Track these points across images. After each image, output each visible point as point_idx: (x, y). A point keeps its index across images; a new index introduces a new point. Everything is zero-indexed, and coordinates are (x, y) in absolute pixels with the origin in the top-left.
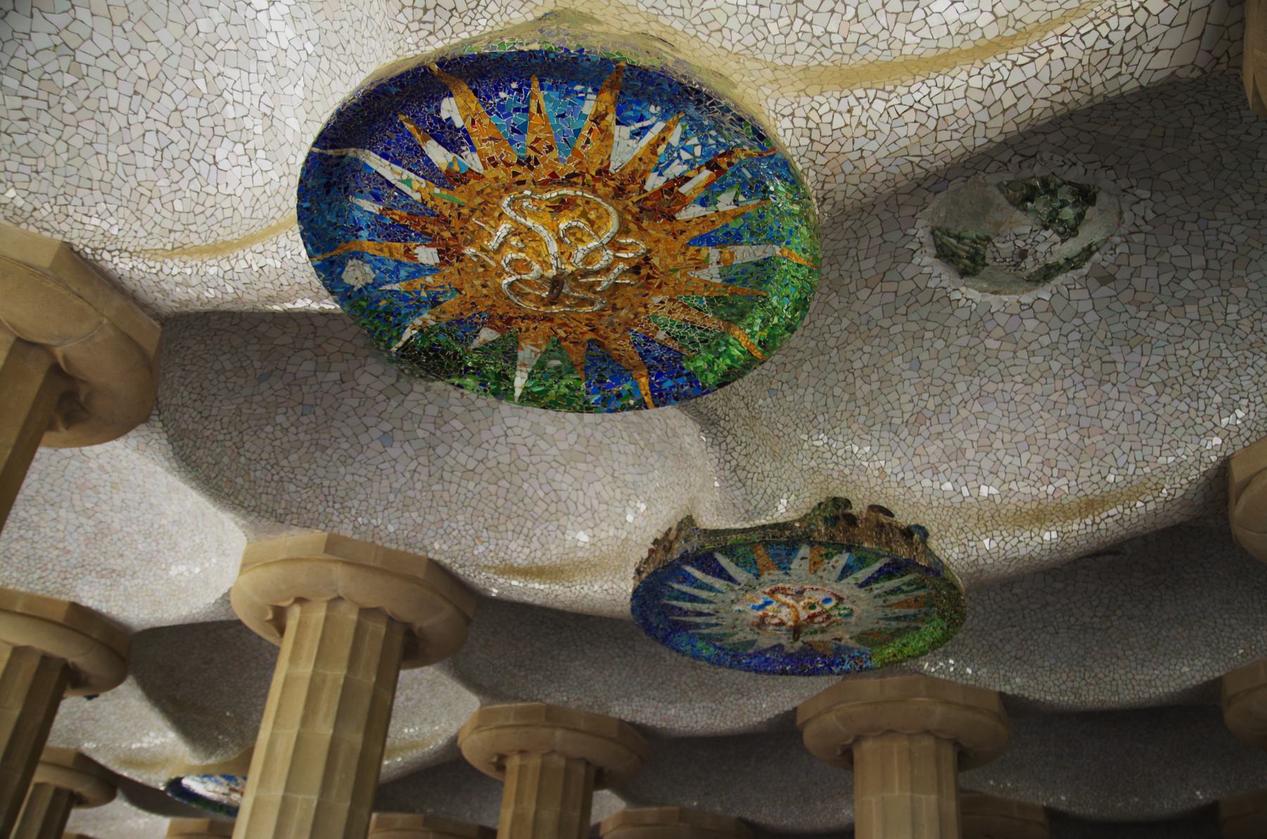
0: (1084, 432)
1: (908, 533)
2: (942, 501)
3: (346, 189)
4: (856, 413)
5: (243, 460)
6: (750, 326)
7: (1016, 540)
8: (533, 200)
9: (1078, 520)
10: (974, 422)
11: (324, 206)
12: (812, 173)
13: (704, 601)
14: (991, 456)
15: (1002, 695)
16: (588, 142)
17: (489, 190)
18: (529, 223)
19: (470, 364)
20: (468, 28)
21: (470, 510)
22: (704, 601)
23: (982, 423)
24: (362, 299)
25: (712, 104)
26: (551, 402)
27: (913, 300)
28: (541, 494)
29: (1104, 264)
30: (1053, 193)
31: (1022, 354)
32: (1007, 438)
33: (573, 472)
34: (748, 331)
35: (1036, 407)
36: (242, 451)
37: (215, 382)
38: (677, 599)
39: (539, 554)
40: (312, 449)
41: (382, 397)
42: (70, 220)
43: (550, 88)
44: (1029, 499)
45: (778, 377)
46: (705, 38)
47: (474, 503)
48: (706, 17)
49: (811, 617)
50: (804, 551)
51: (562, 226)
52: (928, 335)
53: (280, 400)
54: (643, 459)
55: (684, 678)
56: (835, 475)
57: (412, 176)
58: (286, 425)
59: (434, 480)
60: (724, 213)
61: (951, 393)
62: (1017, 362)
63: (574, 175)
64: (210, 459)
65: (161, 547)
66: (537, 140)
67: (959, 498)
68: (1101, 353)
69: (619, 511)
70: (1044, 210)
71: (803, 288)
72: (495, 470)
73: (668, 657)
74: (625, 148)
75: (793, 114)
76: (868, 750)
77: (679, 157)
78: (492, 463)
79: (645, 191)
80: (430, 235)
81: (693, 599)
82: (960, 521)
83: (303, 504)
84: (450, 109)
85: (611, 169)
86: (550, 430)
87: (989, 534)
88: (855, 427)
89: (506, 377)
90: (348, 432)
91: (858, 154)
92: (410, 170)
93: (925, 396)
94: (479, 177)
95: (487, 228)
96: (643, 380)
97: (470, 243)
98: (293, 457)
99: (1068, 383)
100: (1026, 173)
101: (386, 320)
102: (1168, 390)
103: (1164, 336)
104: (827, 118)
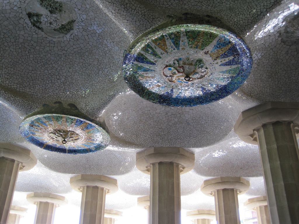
5: (211, 133)
27: (87, 30)
36: (209, 132)
37: (186, 133)
45: (116, 65)
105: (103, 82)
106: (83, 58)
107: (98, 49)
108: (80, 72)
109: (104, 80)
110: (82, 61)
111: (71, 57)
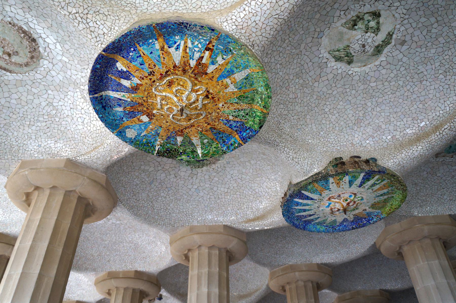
0: (423, 102)
1: (367, 162)
2: (379, 147)
3: (110, 106)
4: (334, 127)
5: (155, 210)
6: (258, 102)
7: (411, 151)
8: (161, 86)
9: (433, 135)
10: (380, 115)
11: (107, 115)
12: (243, 37)
13: (308, 210)
14: (392, 124)
15: (450, 215)
16: (164, 58)
17: (147, 89)
18: (164, 94)
19: (181, 151)
20: (111, 37)
21: (231, 205)
22: (308, 210)
23: (383, 114)
24: (137, 141)
25: (190, 26)
26: (212, 154)
27: (335, 80)
28: (250, 193)
29: (399, 38)
30: (363, 19)
31: (386, 83)
32: (395, 116)
33: (256, 182)
34: (258, 105)
35: (401, 101)
36: (154, 208)
37: (136, 189)
38: (299, 212)
39: (256, 213)
40: (176, 201)
41: (190, 178)
42: (67, 152)
43: (143, 46)
44: (413, 135)
45: (299, 124)
46: (195, 12)
47: (231, 202)
48: (194, 5)
49: (348, 204)
50: (331, 180)
51: (174, 91)
52: (348, 90)
53: (160, 188)
55: (334, 243)
56: (334, 150)
57: (124, 93)
58: (165, 196)
59: (217, 199)
60: (222, 64)
61: (366, 107)
62: (386, 87)
63: (167, 72)
64: (144, 213)
65: (153, 246)
66: (149, 65)
67: (386, 144)
68: (416, 71)
70: (363, 27)
71: (264, 80)
72: (234, 190)
73: (325, 237)
74: (177, 56)
75: (227, 20)
76: (405, 249)
77: (195, 51)
78: (232, 188)
79: (192, 68)
80: (141, 111)
81: (305, 211)
82: (388, 151)
83: (179, 219)
84: (120, 66)
85: (177, 65)
86: (244, 171)
87: (401, 152)
88: (336, 132)
89: (194, 151)
90: (185, 192)
91: (254, 24)
92: (122, 92)
93: (357, 112)
94: (141, 85)
95: (154, 101)
96: (237, 136)
97: (153, 109)
98: (171, 205)
99: (408, 87)
100: (349, 17)
101: (148, 145)
102: (448, 74)
103: (436, 54)
104: (238, 16)
105: (272, 116)
106: (295, 78)
107: (310, 95)
108: (276, 79)
109: (275, 116)
110: (291, 77)
111: (295, 61)
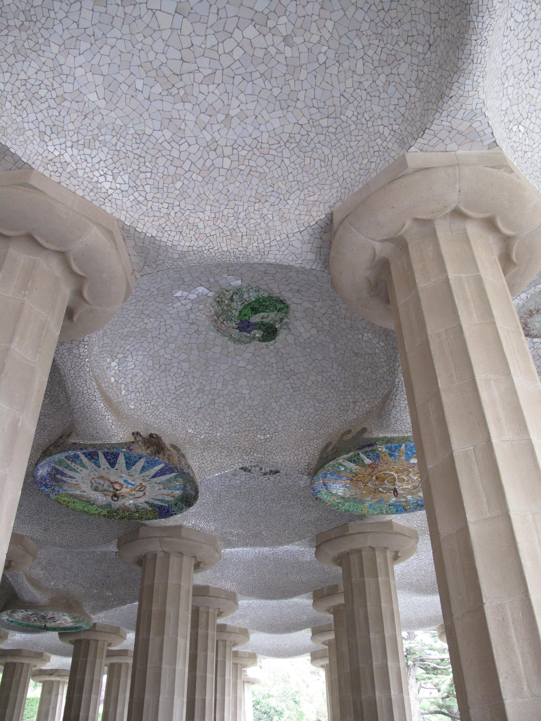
28: (127, 348)
38: (126, 458)
54: (168, 394)
69: (130, 389)
86: (172, 346)
